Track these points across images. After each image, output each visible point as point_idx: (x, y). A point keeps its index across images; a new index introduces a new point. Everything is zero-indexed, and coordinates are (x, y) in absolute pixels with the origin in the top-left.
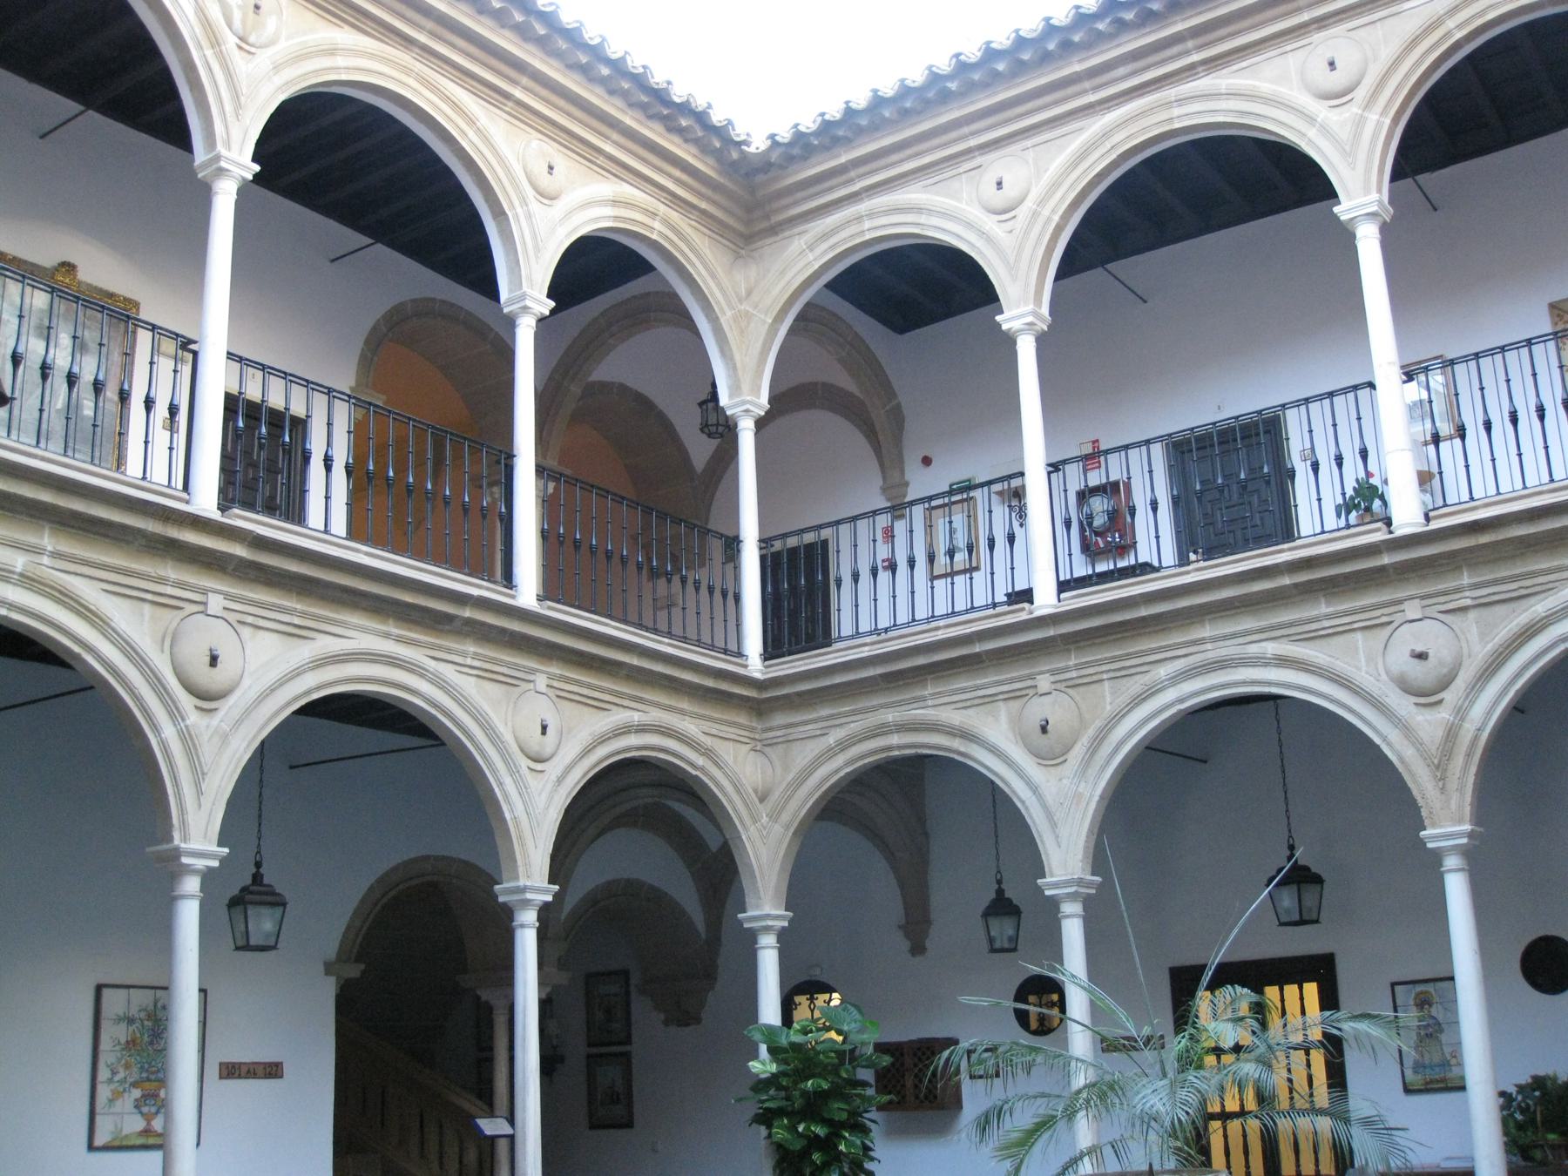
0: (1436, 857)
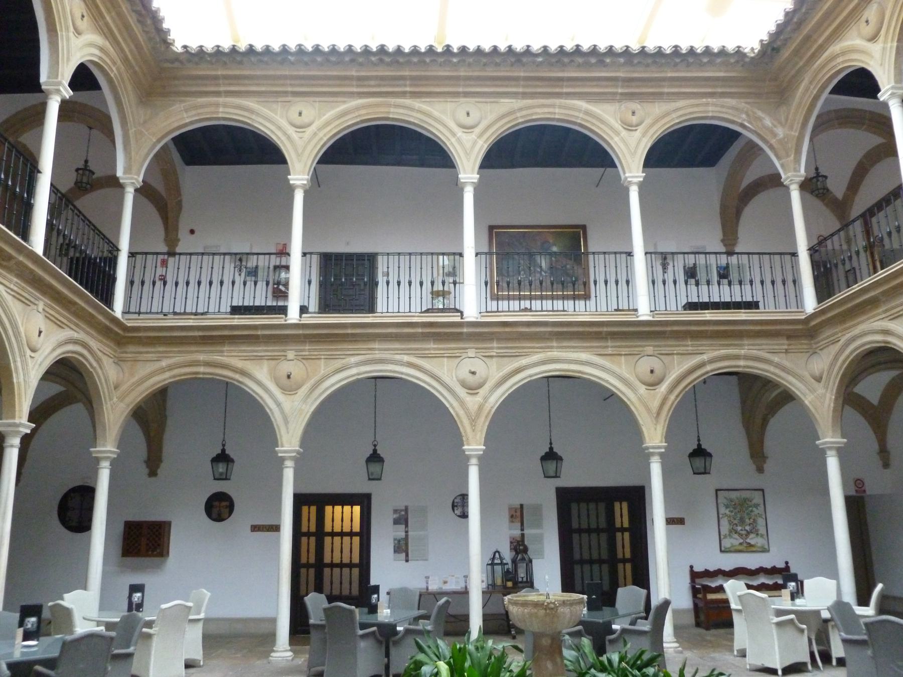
0: (468, 458)
